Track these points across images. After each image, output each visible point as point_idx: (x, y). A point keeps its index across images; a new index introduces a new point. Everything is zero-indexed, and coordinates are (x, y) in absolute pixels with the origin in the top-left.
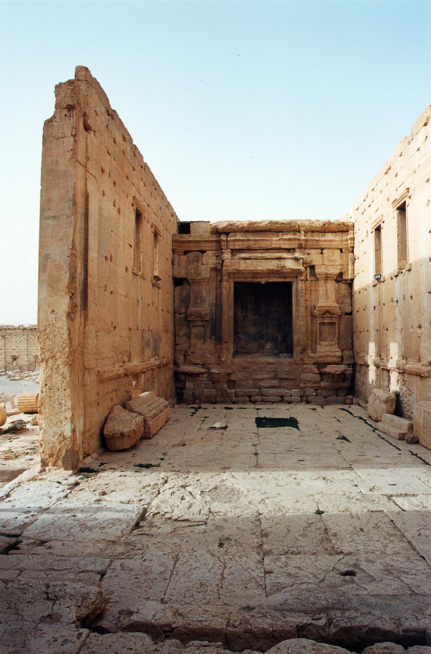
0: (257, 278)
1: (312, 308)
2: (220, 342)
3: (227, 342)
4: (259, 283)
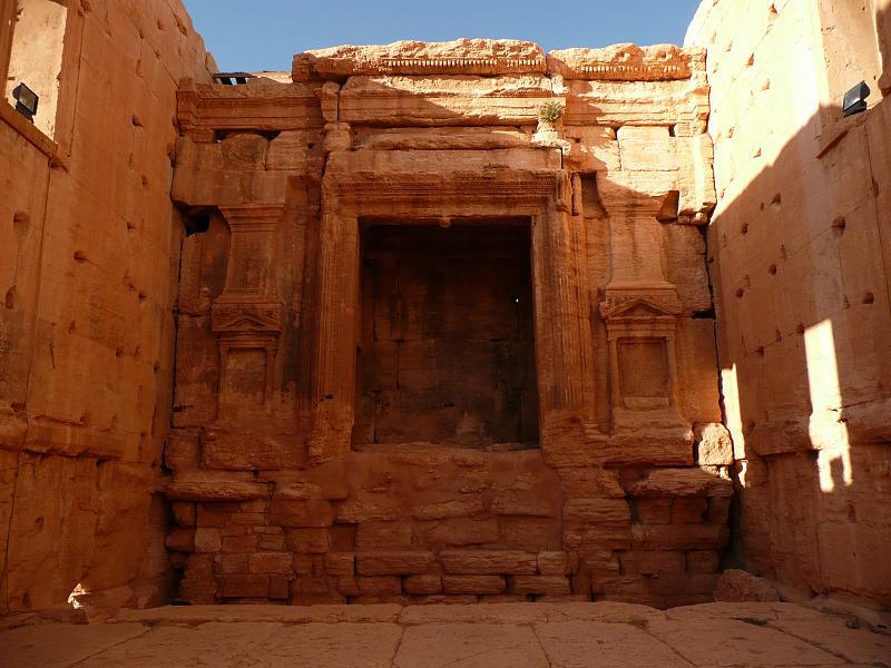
0: (426, 204)
1: (594, 295)
2: (310, 398)
3: (330, 397)
4: (433, 226)
